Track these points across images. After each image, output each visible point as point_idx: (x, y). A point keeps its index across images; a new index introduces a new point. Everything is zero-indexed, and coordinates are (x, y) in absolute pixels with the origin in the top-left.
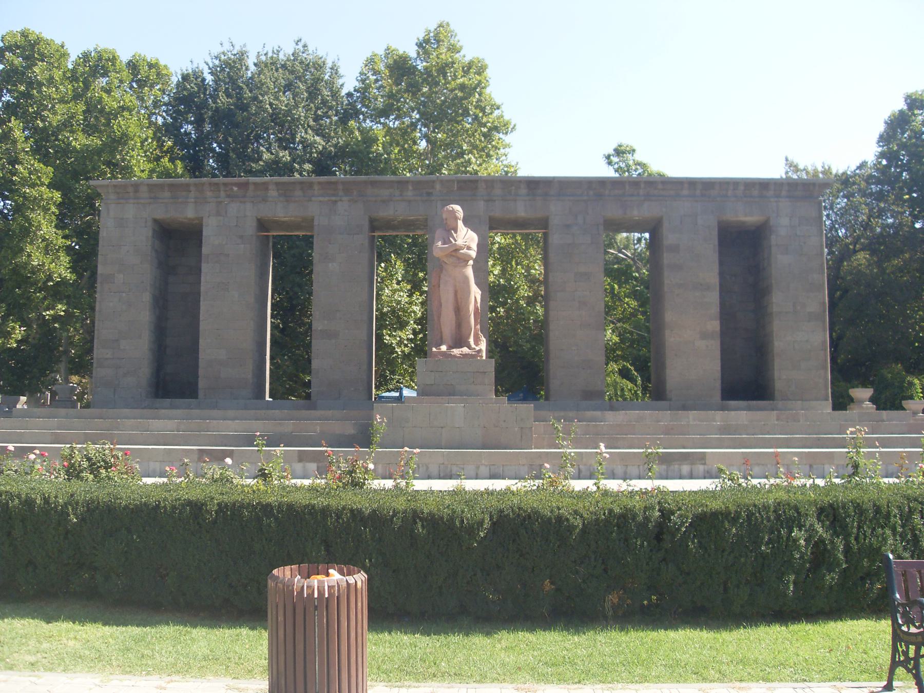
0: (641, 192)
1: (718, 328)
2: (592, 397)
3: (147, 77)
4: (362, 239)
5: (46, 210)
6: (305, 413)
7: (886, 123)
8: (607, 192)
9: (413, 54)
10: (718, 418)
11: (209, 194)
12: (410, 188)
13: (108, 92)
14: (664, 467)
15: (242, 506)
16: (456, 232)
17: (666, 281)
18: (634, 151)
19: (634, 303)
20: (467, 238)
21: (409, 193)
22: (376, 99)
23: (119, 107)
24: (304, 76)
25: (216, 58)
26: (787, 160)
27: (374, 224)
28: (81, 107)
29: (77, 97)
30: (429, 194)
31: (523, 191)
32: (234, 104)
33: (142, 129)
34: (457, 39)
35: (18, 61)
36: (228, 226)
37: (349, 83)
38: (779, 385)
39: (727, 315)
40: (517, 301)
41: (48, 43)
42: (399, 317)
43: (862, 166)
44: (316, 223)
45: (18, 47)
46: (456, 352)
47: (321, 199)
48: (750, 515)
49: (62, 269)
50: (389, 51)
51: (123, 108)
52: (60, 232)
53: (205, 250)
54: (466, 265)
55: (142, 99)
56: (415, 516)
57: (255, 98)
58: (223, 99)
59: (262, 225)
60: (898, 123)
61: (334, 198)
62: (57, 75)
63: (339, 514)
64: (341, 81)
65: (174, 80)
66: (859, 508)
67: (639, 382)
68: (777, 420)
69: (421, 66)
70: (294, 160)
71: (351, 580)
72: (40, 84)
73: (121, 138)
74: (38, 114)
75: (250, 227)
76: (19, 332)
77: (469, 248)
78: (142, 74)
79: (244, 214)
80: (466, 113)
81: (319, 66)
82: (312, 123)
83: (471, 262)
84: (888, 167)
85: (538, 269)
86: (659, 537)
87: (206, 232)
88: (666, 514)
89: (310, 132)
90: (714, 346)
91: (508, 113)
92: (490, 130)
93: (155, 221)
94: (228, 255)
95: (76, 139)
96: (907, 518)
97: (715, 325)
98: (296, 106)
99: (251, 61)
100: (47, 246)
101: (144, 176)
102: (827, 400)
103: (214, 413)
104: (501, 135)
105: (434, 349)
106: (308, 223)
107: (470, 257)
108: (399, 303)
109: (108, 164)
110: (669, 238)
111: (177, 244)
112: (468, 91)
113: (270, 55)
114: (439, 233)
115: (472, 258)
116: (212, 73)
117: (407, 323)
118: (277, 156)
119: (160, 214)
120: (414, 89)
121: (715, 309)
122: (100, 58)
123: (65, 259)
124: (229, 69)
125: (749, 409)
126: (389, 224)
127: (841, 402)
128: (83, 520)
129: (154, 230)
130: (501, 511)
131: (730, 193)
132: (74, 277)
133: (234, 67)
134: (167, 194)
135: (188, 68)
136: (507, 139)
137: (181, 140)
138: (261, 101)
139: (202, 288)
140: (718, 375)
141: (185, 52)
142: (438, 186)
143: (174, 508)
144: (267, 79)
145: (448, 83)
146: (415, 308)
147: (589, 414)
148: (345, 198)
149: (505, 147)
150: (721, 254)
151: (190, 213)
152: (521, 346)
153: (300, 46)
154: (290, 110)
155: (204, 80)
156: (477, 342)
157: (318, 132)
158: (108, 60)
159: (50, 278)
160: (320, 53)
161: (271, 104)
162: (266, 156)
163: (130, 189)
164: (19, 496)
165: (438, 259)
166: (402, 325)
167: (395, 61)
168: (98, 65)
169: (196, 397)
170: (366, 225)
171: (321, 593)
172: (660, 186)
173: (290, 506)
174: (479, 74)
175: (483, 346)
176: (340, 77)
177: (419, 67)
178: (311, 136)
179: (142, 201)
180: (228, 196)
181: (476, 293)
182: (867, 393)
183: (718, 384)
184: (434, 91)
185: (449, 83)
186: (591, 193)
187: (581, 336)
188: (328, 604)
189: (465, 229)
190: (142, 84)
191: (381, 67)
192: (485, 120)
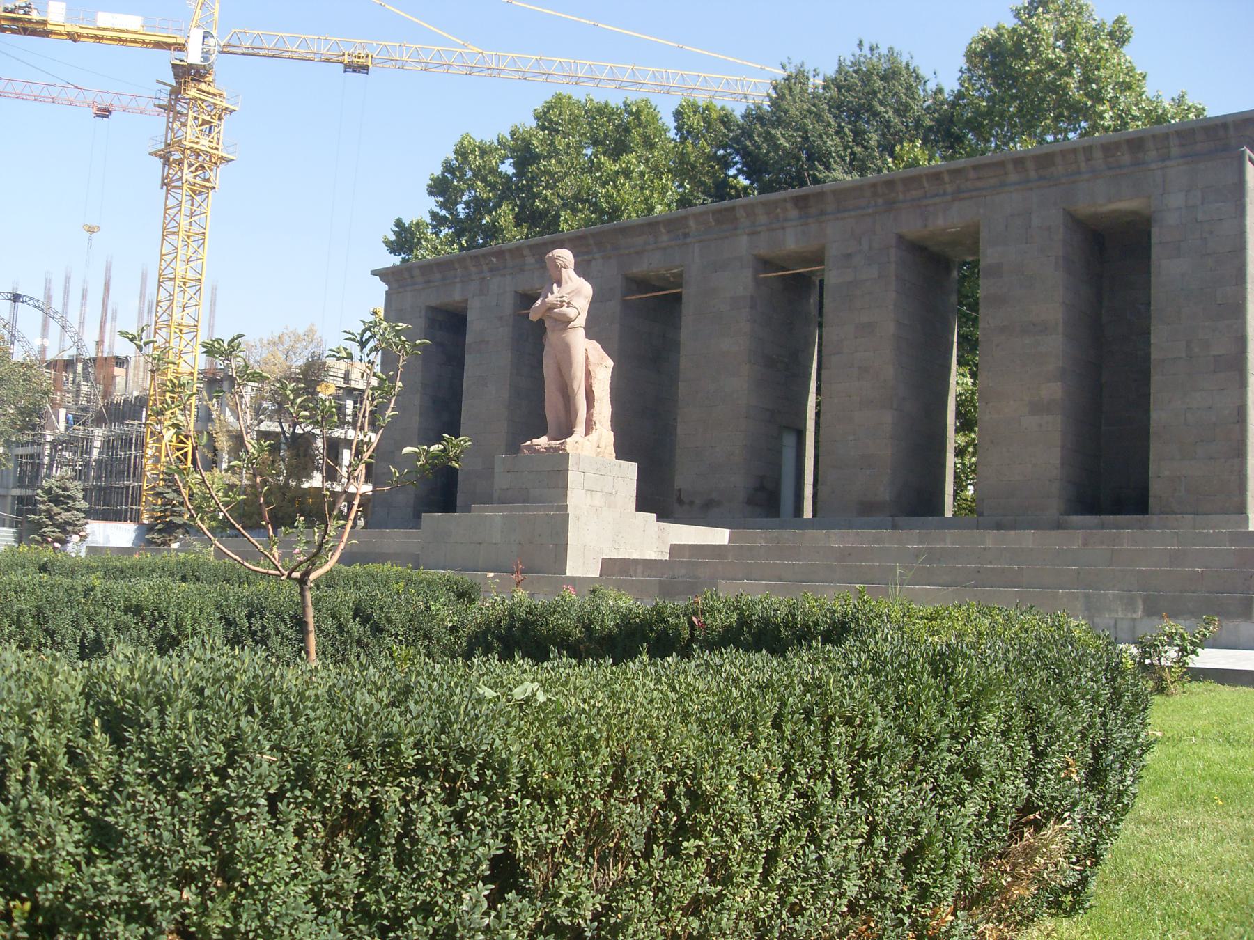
0: (949, 188)
10: (1054, 541)
11: (473, 269)
30: (686, 235)
38: (1155, 487)
53: (469, 339)
77: (569, 305)
83: (581, 321)
87: (471, 317)
93: (433, 309)
97: (1054, 390)
119: (434, 301)
125: (1102, 526)
131: (1083, 165)
134: (438, 276)
142: (692, 223)
148: (597, 256)
151: (457, 297)
153: (866, 51)
172: (972, 175)
179: (417, 287)
180: (491, 270)
186: (880, 201)
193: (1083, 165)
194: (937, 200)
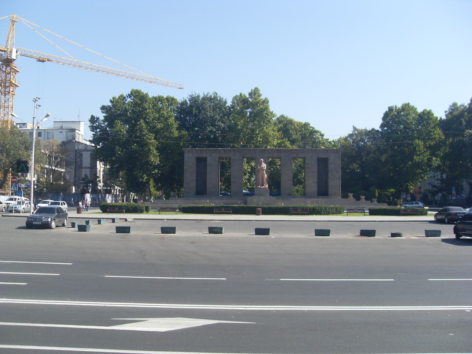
5: (154, 146)
9: (248, 96)
36: (213, 157)
37: (229, 104)
40: (276, 167)
60: (386, 115)
72: (146, 109)
87: (208, 160)
90: (316, 185)
97: (316, 180)
110: (307, 162)
112: (262, 110)
116: (189, 101)
117: (247, 174)
119: (198, 156)
121: (316, 177)
124: (194, 100)
127: (345, 196)
151: (204, 156)
175: (267, 186)
178: (220, 123)
181: (266, 175)
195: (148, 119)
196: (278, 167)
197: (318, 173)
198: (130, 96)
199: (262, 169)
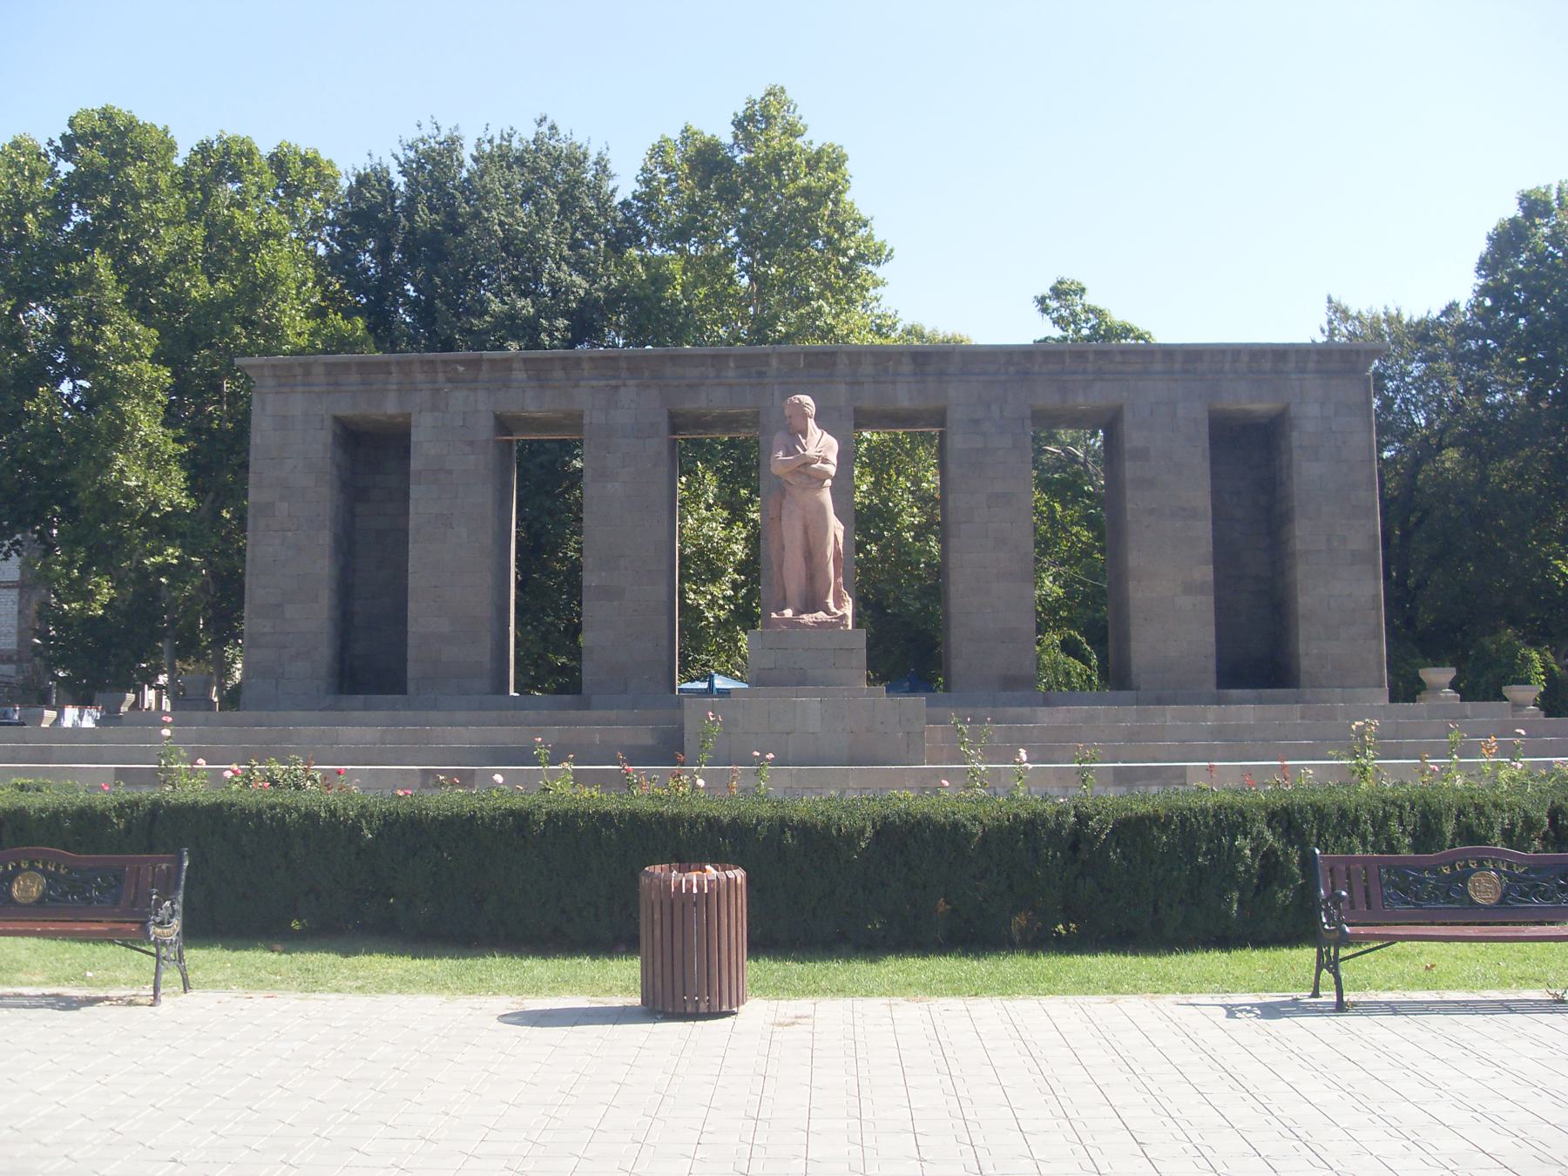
1: (1210, 577)
2: (1017, 685)
3: (301, 180)
4: (658, 445)
5: (148, 397)
6: (573, 714)
7: (1490, 238)
8: (1036, 368)
10: (1211, 715)
11: (420, 377)
12: (732, 365)
13: (241, 205)
14: (1123, 790)
15: (576, 815)
16: (805, 437)
17: (1129, 506)
18: (1083, 290)
19: (1086, 535)
20: (821, 445)
21: (731, 373)
22: (668, 212)
23: (263, 232)
24: (551, 174)
25: (411, 147)
26: (1330, 301)
27: (677, 423)
28: (199, 232)
29: (194, 213)
30: (761, 374)
31: (907, 367)
32: (444, 224)
33: (296, 265)
34: (797, 114)
35: (101, 160)
36: (451, 427)
37: (624, 185)
38: (1305, 664)
39: (1225, 558)
40: (899, 533)
41: (147, 130)
42: (709, 562)
43: (1451, 309)
44: (586, 421)
45: (97, 136)
46: (807, 618)
47: (594, 383)
48: (1184, 820)
49: (173, 492)
50: (687, 134)
51: (267, 234)
52: (170, 432)
53: (415, 464)
54: (822, 486)
55: (293, 216)
56: (784, 823)
57: (476, 215)
58: (424, 217)
59: (503, 424)
60: (1508, 240)
61: (613, 382)
62: (163, 180)
63: (693, 823)
64: (611, 185)
65: (344, 184)
66: (1320, 813)
67: (1094, 662)
68: (1303, 717)
69: (741, 158)
70: (538, 314)
71: (731, 874)
72: (137, 197)
73: (266, 281)
74: (133, 245)
75: (484, 429)
76: (106, 591)
77: (825, 461)
78: (293, 174)
79: (475, 407)
80: (814, 233)
81: (576, 160)
82: (566, 252)
83: (828, 482)
84: (1493, 310)
85: (931, 481)
86: (1075, 847)
87: (415, 437)
88: (1082, 819)
89: (565, 268)
90: (1207, 602)
91: (881, 232)
92: (852, 260)
94: (450, 472)
95: (195, 286)
96: (1381, 824)
97: (1206, 573)
98: (542, 226)
99: (467, 152)
100: (150, 455)
101: (303, 342)
102: (1381, 686)
103: (434, 715)
104: (870, 267)
105: (774, 615)
106: (574, 421)
107: (827, 475)
108: (709, 539)
109: (246, 323)
110: (1133, 438)
111: (371, 456)
112: (818, 197)
113: (497, 141)
114: (779, 438)
115: (830, 477)
116: (404, 173)
117: (723, 572)
118: (513, 307)
119: (345, 409)
120: (729, 195)
121: (1206, 547)
122: (227, 152)
123: (178, 476)
124: (432, 164)
125: (1259, 701)
126: (700, 422)
127: (1406, 689)
128: (379, 835)
129: (335, 434)
130: (886, 817)
131: (1227, 367)
132: (192, 504)
133: (439, 162)
134: (354, 378)
135: (362, 165)
136: (880, 272)
137: (356, 280)
138: (487, 220)
139: (412, 524)
140: (1211, 649)
141: (360, 139)
142: (774, 363)
143: (493, 818)
144: (494, 182)
145: (783, 185)
146: (735, 547)
147: (1013, 711)
148: (631, 382)
149: (876, 285)
150: (1214, 463)
151: (391, 407)
152: (907, 605)
153: (545, 129)
154: (532, 233)
155: (390, 183)
156: (839, 603)
157: (579, 266)
158: (240, 155)
159: (154, 506)
160: (578, 139)
161: (501, 224)
162: (496, 306)
163: (298, 371)
164: (297, 809)
165: (778, 477)
166: (716, 575)
167: (699, 151)
168: (224, 161)
169: (404, 692)
170: (664, 426)
171: (700, 888)
172: (1119, 358)
173: (634, 816)
174: (834, 170)
175: (848, 609)
176: (610, 177)
177: (738, 160)
179: (316, 389)
180: (449, 380)
181: (836, 528)
182: (1449, 673)
183: (1211, 665)
184: (762, 199)
185: (785, 186)
186: (1012, 369)
187: (999, 588)
188: (707, 900)
189: (819, 432)
190: (292, 191)
191: (676, 158)
192: (844, 244)
193: (1227, 367)
194: (1079, 377)
195: (141, 251)
196: (909, 536)
197: (1220, 516)
198: (68, 147)
199: (807, 473)
